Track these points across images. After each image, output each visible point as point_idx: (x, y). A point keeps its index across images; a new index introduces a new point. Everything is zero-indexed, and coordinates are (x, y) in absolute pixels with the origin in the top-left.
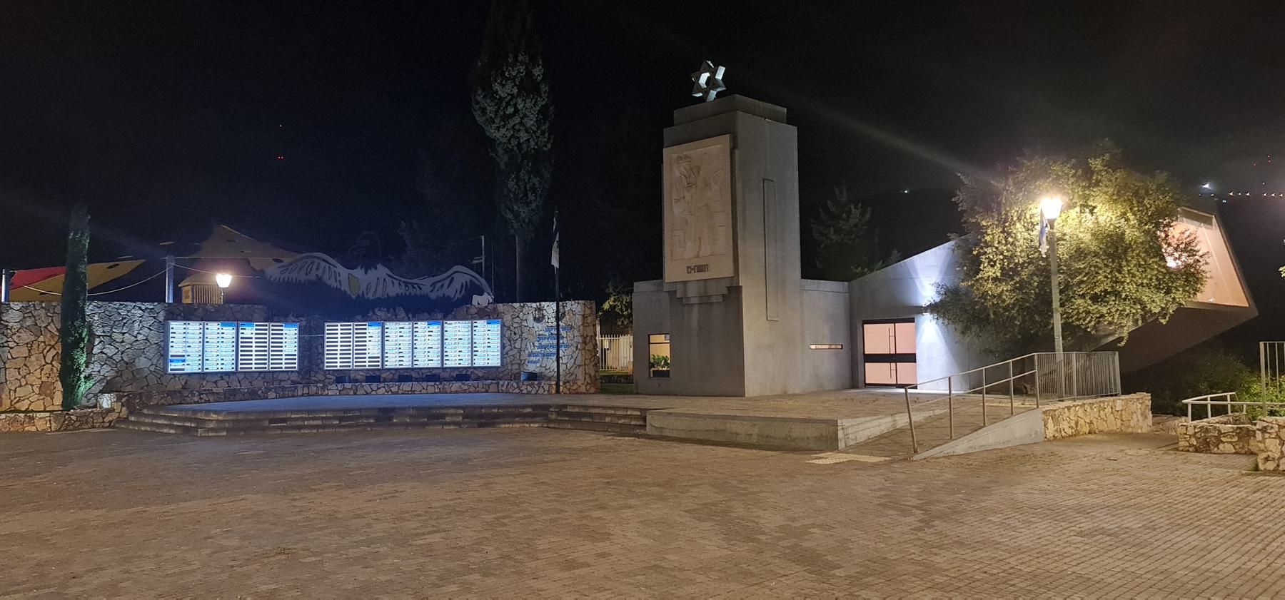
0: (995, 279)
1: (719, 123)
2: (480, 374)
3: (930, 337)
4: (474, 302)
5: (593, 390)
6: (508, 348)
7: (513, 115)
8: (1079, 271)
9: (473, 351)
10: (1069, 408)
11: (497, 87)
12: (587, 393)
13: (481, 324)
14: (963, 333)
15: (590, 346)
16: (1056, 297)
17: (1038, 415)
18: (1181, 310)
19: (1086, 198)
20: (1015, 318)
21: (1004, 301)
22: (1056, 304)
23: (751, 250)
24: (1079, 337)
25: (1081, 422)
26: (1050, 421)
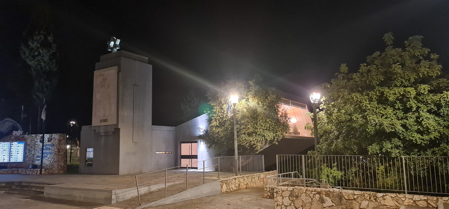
0: (217, 126)
1: (115, 61)
2: (14, 165)
3: (202, 148)
4: (14, 134)
5: (62, 172)
6: (28, 154)
7: (38, 56)
8: (243, 124)
9: (10, 156)
10: (235, 179)
11: (30, 43)
12: (58, 174)
13: (15, 144)
14: (209, 147)
15: (62, 153)
16: (236, 134)
17: (218, 183)
18: (284, 139)
19: (247, 95)
20: (224, 142)
21: (220, 135)
22: (235, 137)
23: (126, 113)
24: (243, 150)
25: (242, 184)
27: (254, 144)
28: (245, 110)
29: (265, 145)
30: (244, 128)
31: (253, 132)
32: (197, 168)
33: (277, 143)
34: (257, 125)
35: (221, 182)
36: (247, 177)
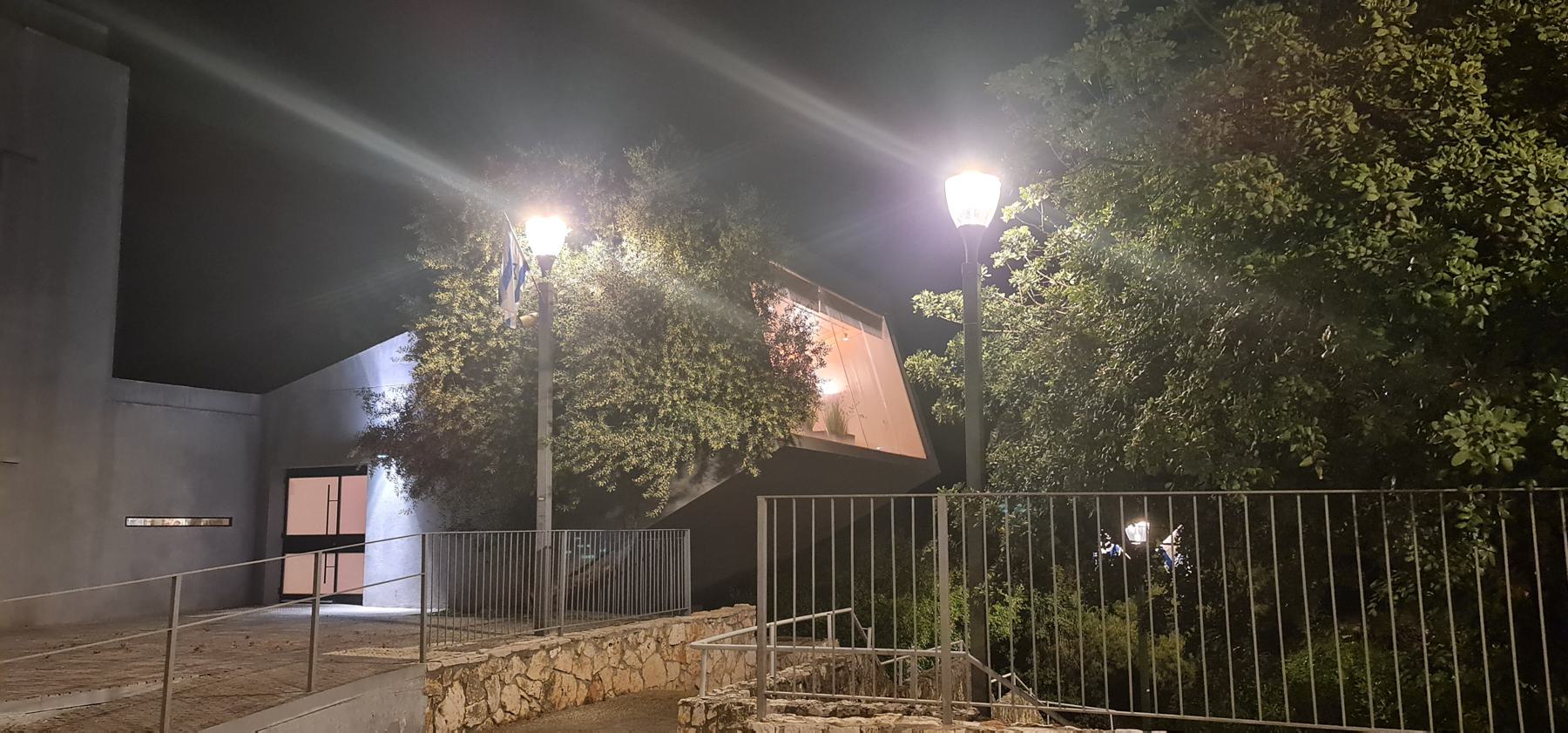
3: (388, 502)
8: (586, 363)
10: (525, 655)
16: (545, 414)
22: (544, 432)
24: (582, 504)
26: (457, 691)
27: (638, 470)
28: (597, 291)
29: (698, 478)
30: (591, 385)
31: (639, 409)
32: (357, 600)
33: (755, 472)
34: (657, 367)
35: (432, 675)
36: (598, 643)
